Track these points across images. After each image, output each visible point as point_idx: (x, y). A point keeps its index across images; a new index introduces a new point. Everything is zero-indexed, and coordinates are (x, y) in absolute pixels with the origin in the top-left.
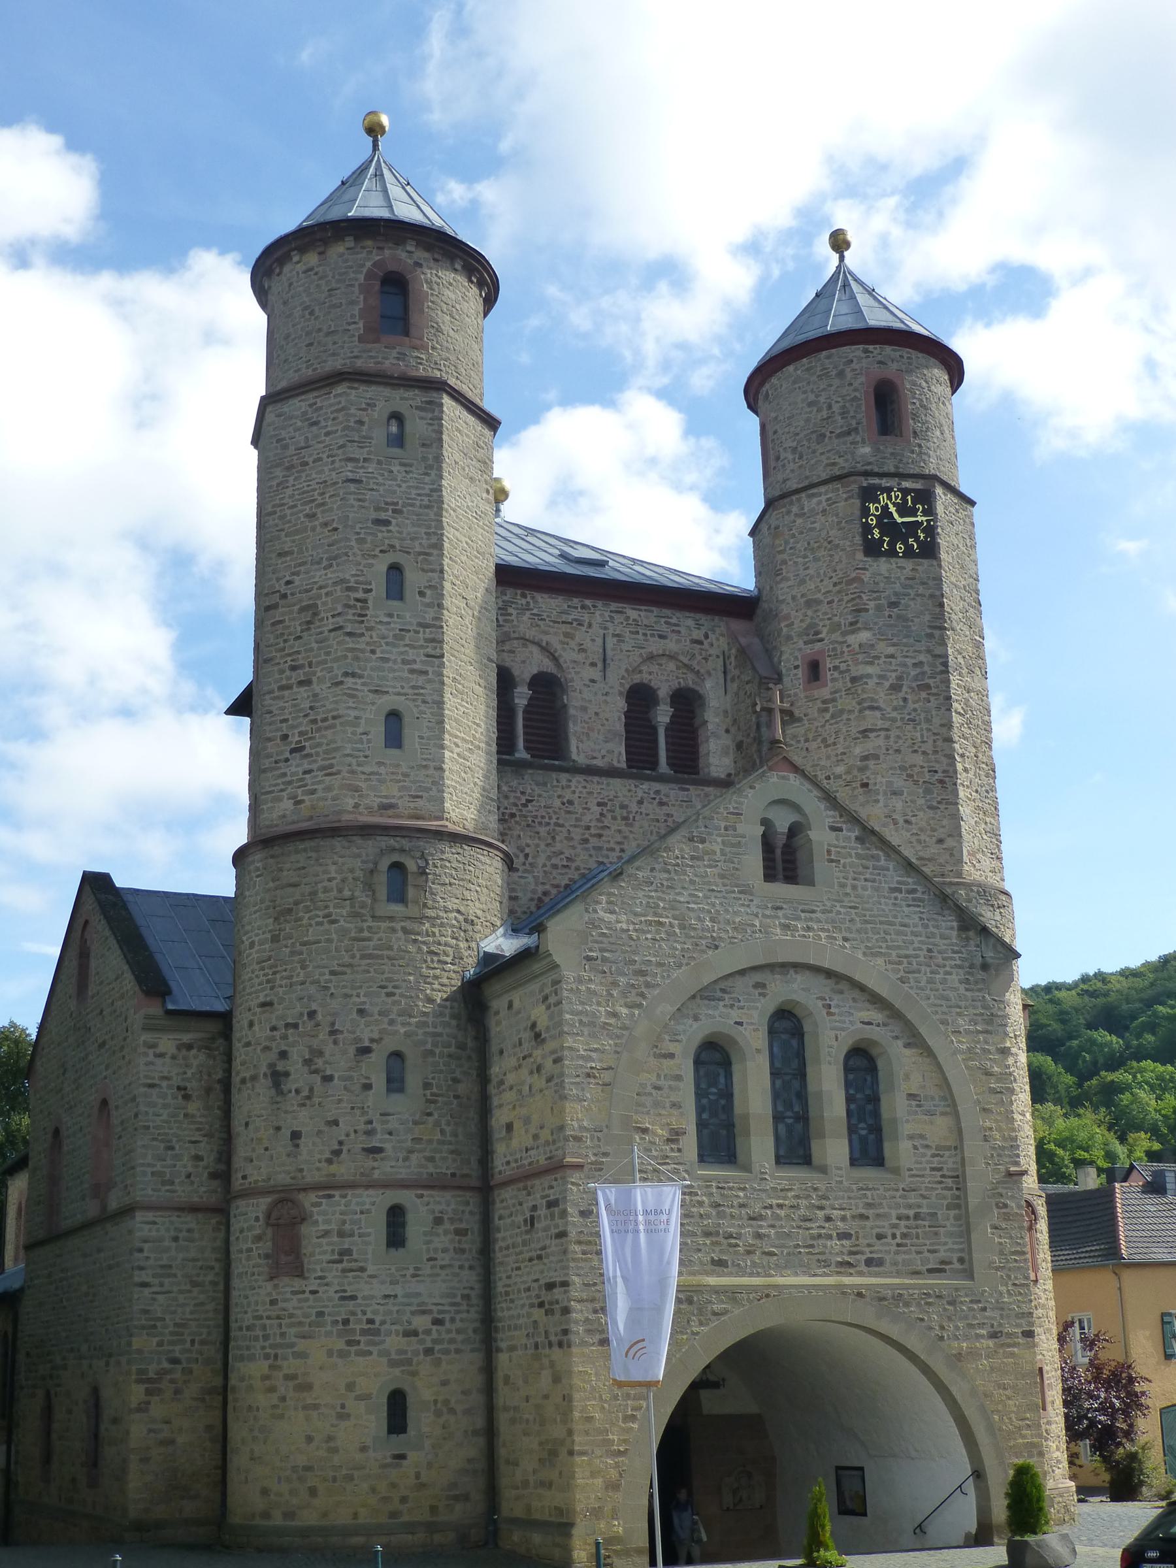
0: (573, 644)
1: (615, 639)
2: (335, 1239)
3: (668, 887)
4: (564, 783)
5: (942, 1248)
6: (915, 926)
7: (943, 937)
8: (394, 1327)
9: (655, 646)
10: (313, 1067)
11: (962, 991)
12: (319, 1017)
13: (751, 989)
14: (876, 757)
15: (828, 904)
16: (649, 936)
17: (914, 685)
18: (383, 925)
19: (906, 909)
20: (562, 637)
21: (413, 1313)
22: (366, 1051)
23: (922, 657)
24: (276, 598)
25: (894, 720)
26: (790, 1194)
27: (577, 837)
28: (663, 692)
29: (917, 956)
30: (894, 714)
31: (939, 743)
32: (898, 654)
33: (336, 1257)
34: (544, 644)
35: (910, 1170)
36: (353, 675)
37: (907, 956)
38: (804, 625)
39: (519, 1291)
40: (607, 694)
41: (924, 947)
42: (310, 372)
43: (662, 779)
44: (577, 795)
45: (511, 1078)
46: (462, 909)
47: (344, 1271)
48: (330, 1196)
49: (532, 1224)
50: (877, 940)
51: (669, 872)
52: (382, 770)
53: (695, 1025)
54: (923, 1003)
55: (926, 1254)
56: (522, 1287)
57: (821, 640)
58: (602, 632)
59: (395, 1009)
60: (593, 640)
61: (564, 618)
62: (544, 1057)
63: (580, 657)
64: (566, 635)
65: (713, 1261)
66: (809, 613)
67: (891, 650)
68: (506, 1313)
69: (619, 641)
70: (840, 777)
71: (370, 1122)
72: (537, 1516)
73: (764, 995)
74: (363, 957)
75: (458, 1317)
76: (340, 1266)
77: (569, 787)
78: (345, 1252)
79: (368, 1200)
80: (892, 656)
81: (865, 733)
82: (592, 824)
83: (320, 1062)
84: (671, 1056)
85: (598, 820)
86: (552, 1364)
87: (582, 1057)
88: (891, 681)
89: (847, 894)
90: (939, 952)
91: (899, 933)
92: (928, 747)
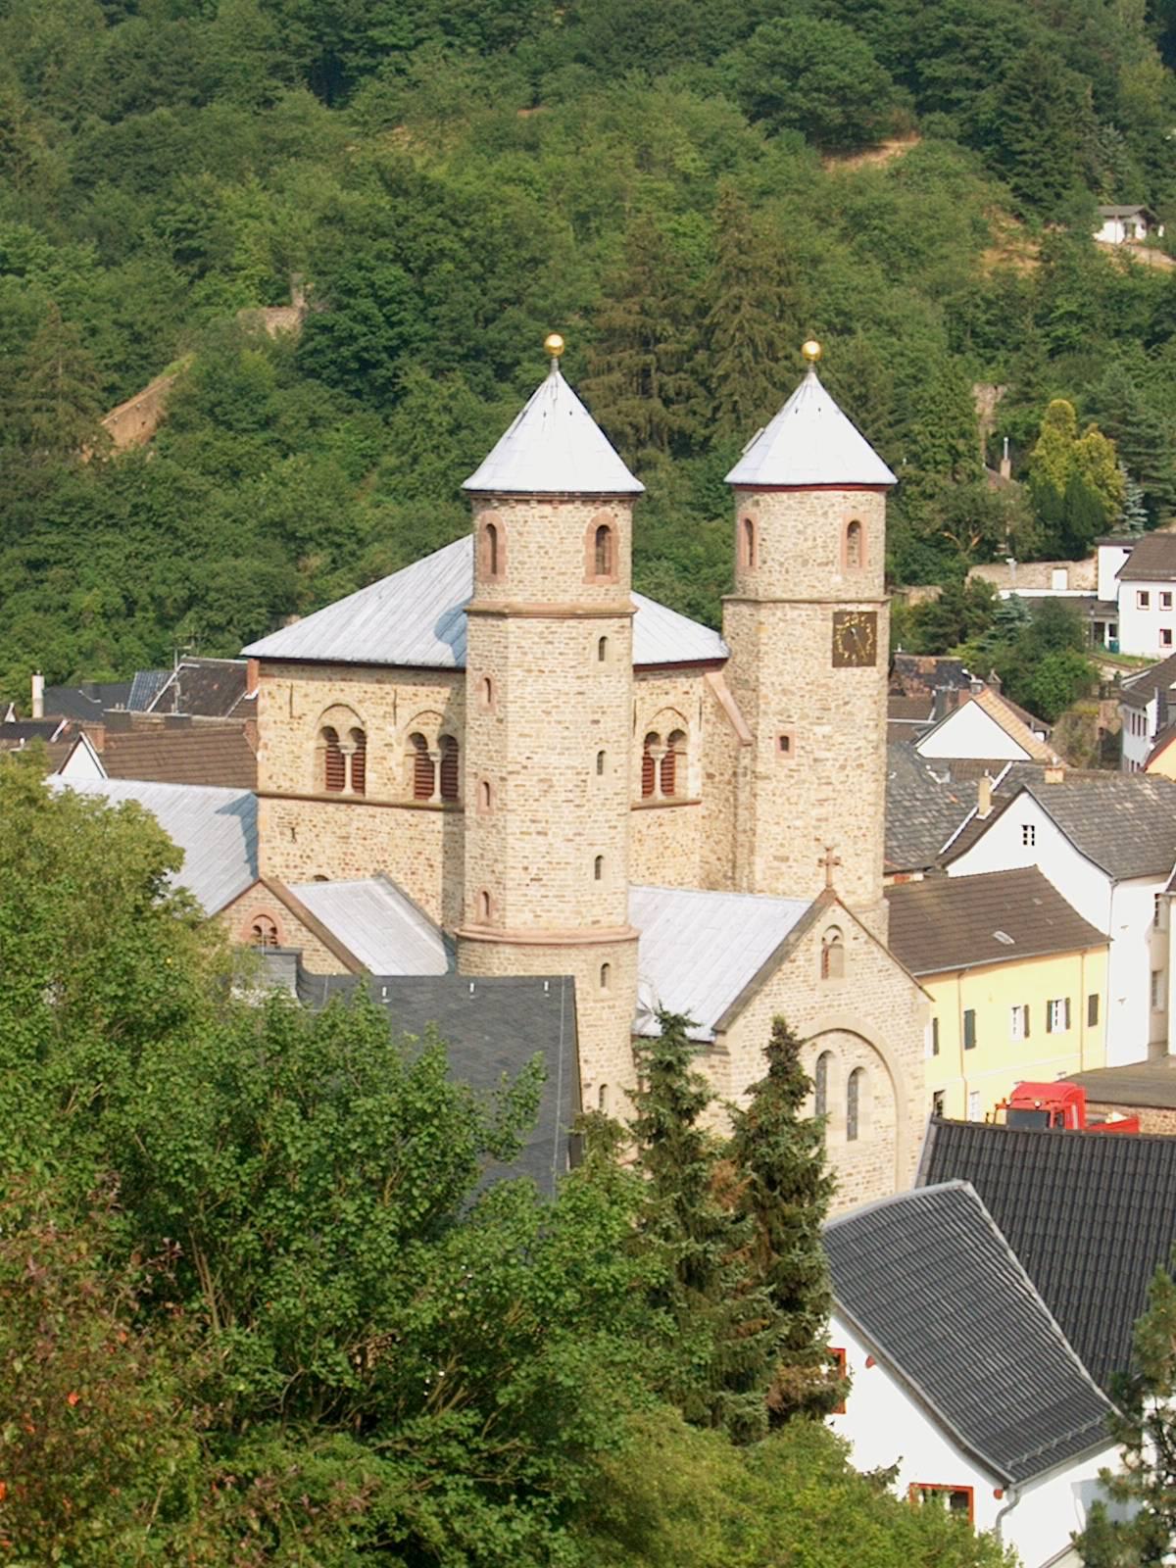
14: (826, 820)
23: (861, 743)
24: (518, 767)
36: (580, 834)
38: (779, 707)
42: (545, 600)
52: (594, 898)
66: (784, 699)
67: (841, 739)
70: (797, 828)
81: (821, 802)
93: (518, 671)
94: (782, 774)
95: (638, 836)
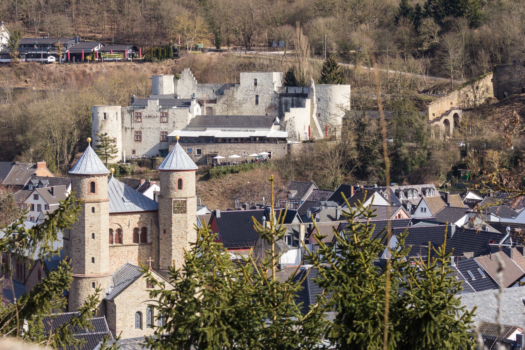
94: (164, 239)
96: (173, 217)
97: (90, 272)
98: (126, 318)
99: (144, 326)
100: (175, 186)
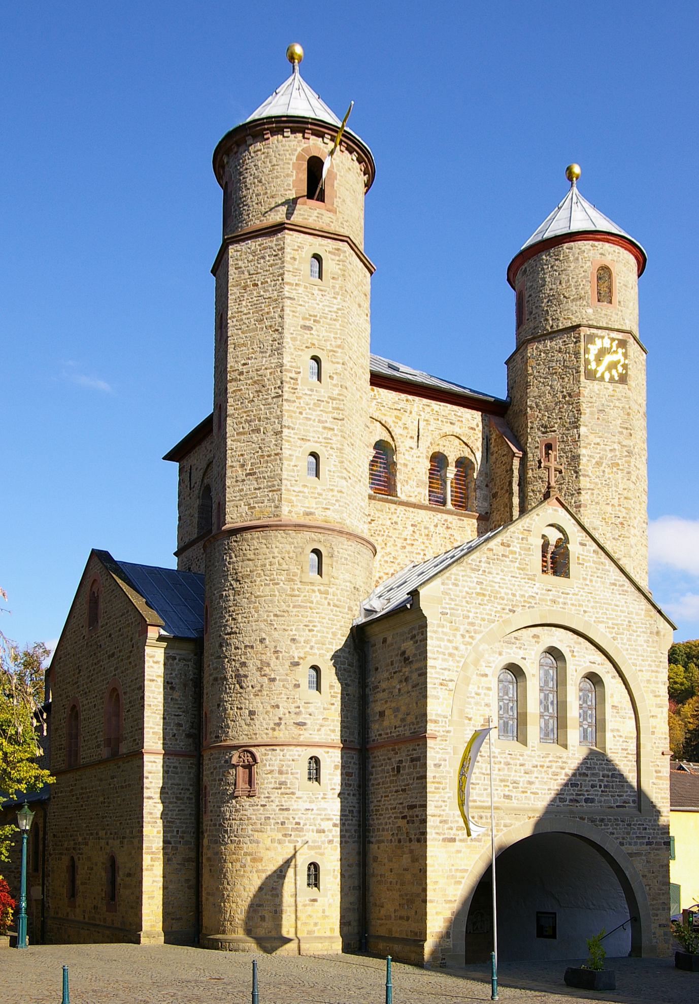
0: (400, 423)
1: (425, 423)
2: (277, 775)
3: (489, 573)
4: (393, 510)
5: (625, 794)
6: (622, 606)
7: (637, 614)
8: (311, 828)
9: (448, 429)
10: (263, 673)
11: (645, 647)
12: (267, 642)
13: (531, 639)
15: (577, 590)
16: (478, 602)
17: (610, 463)
18: (307, 588)
19: (618, 596)
20: (394, 419)
21: (322, 820)
22: (297, 664)
25: (596, 484)
26: (548, 760)
27: (399, 545)
28: (452, 459)
29: (622, 625)
30: (597, 480)
31: (622, 500)
32: (601, 443)
33: (278, 786)
34: (383, 422)
35: (611, 749)
37: (617, 624)
39: (387, 809)
40: (419, 457)
41: (627, 620)
43: (449, 512)
44: (400, 519)
45: (384, 685)
46: (353, 581)
47: (282, 794)
48: (273, 750)
49: (398, 771)
50: (602, 614)
51: (489, 563)
53: (500, 658)
54: (625, 653)
55: (617, 797)
56: (389, 807)
57: (555, 431)
58: (418, 417)
59: (314, 639)
60: (412, 422)
61: (396, 406)
62: (411, 672)
63: (404, 432)
64: (397, 417)
65: (504, 795)
68: (376, 822)
69: (427, 424)
71: (299, 707)
72: (395, 935)
73: (538, 642)
74: (294, 607)
75: (346, 823)
76: (280, 791)
77: (396, 513)
78: (284, 783)
79: (297, 753)
80: (598, 444)
82: (408, 537)
83: (267, 670)
84: (486, 675)
85: (412, 535)
86: (411, 851)
87: (438, 673)
88: (596, 459)
89: (587, 585)
90: (635, 623)
91: (613, 610)
92: (616, 502)
93: (235, 290)
95: (424, 532)
96: (585, 392)
97: (302, 510)
98: (467, 681)
99: (533, 731)
100: (589, 288)
